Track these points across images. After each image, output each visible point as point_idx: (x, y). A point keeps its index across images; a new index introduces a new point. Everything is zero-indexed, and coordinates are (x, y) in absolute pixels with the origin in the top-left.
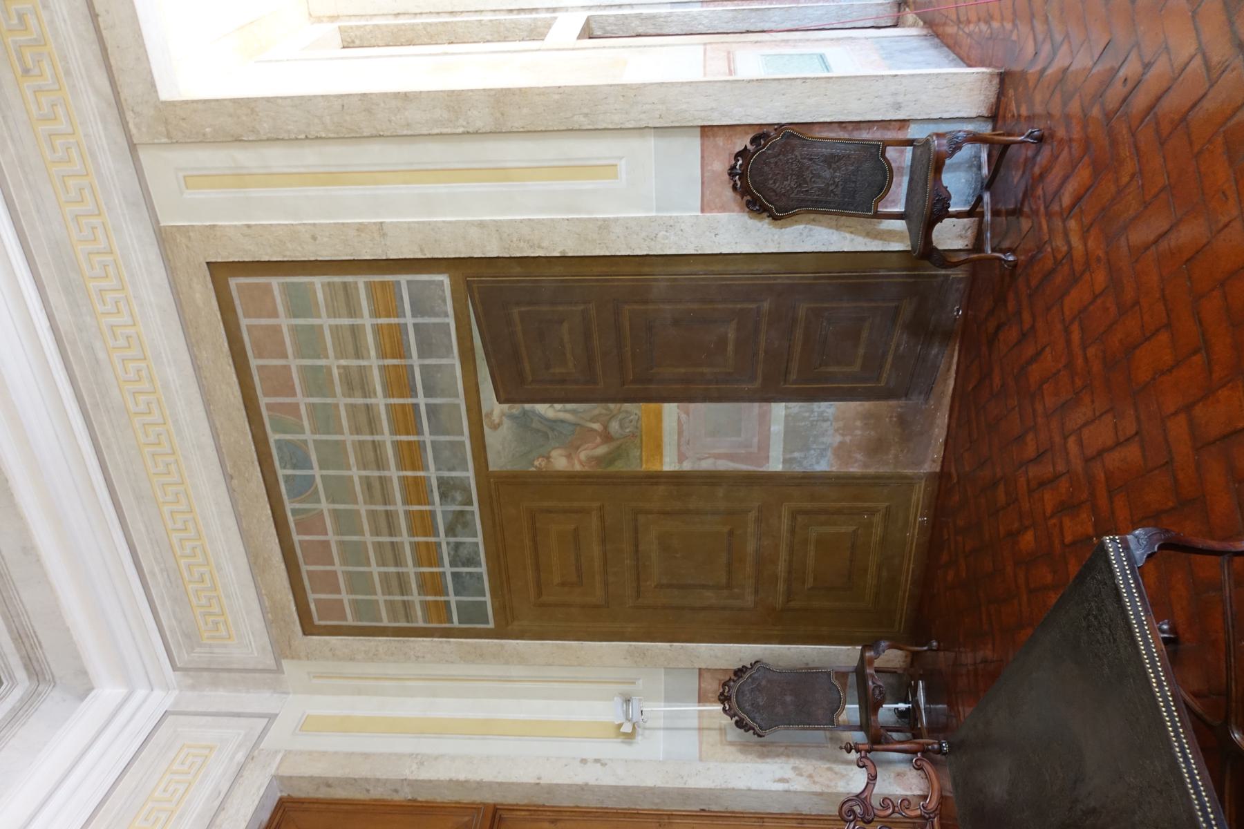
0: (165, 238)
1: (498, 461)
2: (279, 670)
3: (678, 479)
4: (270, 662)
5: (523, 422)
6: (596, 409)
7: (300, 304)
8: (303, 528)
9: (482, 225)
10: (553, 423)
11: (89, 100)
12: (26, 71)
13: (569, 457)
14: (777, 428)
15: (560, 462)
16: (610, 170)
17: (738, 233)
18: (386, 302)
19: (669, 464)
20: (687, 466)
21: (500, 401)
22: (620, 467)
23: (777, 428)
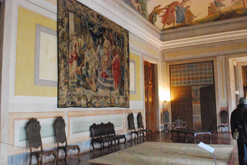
0: (216, 56)
1: (193, 87)
2: (164, 61)
3: (192, 106)
4: (165, 61)
5: (197, 90)
6: (199, 97)
7: (209, 69)
8: (183, 66)
9: (218, 87)
10: (198, 93)
11: (228, 52)
12: (231, 46)
13: (194, 95)
14: (198, 115)
15: (193, 94)
16: (224, 99)
17: (218, 110)
18: (210, 77)
19: (193, 105)
20: (193, 107)
21: (200, 88)
22: (193, 100)
23: (198, 115)
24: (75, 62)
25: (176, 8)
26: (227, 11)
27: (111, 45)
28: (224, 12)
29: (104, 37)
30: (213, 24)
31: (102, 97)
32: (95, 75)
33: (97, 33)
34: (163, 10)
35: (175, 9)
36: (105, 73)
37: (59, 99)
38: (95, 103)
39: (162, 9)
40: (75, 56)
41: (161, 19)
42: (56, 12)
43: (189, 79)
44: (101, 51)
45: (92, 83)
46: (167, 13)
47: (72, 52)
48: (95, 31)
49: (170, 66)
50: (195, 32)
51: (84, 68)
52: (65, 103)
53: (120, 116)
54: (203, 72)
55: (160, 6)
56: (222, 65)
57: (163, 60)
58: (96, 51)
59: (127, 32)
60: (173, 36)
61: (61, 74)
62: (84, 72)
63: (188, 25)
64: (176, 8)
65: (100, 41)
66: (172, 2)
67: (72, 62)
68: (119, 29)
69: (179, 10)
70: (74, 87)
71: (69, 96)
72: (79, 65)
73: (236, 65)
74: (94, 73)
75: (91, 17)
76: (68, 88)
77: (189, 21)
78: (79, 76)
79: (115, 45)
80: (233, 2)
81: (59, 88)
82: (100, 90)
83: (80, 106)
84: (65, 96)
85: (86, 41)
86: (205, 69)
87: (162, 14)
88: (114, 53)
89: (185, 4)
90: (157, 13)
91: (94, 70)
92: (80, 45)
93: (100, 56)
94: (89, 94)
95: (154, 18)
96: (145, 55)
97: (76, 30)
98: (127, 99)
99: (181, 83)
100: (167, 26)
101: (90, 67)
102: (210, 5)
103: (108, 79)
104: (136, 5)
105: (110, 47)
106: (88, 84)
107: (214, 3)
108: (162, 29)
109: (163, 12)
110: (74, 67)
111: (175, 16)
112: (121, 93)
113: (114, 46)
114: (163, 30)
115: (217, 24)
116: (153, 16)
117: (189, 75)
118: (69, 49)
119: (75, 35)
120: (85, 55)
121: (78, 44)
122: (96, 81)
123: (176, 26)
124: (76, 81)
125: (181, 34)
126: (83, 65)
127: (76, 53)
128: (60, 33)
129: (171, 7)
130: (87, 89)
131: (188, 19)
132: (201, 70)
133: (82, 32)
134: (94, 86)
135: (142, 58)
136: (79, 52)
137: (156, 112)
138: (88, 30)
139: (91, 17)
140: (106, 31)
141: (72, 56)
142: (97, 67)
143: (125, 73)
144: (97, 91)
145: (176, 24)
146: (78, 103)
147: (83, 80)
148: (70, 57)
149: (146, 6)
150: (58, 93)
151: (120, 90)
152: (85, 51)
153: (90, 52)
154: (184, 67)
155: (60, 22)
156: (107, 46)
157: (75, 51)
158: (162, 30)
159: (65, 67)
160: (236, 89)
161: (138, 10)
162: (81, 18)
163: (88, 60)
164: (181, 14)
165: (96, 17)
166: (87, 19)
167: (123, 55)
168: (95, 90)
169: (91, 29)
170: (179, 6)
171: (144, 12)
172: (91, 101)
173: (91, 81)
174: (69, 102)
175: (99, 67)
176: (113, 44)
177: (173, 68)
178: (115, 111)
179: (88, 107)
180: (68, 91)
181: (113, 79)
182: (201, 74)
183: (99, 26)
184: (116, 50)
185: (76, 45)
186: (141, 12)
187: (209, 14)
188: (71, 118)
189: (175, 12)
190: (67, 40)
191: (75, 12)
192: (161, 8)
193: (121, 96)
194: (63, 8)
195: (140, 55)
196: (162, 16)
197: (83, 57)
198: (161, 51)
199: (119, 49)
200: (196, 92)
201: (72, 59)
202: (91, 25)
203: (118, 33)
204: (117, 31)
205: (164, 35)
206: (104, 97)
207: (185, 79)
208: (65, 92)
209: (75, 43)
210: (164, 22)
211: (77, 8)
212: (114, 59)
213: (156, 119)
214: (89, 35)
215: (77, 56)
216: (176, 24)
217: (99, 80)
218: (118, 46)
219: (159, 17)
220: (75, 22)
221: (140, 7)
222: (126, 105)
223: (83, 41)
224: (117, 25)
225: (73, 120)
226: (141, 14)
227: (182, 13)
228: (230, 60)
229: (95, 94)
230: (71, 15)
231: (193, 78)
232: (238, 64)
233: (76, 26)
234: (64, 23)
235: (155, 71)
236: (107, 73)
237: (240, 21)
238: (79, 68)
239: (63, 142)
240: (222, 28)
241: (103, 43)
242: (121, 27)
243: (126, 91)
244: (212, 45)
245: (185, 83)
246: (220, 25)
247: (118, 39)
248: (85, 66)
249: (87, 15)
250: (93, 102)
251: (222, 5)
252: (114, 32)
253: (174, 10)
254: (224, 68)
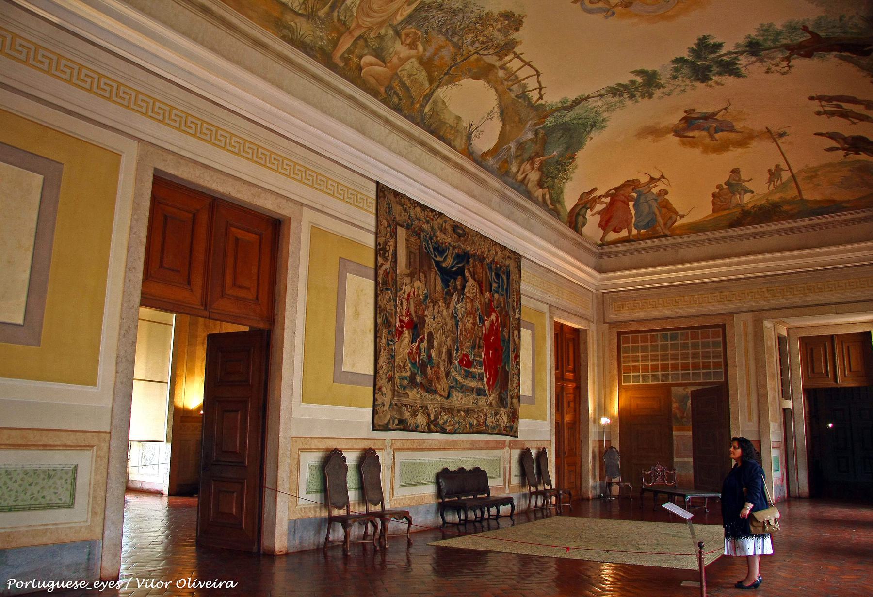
0: (731, 314)
1: (674, 389)
2: (604, 323)
3: (671, 435)
4: (607, 320)
6: (690, 415)
7: (715, 344)
8: (652, 336)
11: (762, 303)
13: (678, 408)
14: (686, 460)
15: (674, 405)
16: (750, 419)
18: (717, 365)
23: (686, 460)
24: (406, 334)
25: (635, 195)
26: (759, 204)
27: (481, 292)
28: (750, 206)
29: (467, 274)
30: (725, 234)
31: (459, 411)
33: (452, 267)
34: (603, 199)
35: (632, 197)
36: (466, 355)
37: (375, 413)
38: (445, 422)
39: (600, 197)
40: (406, 319)
41: (598, 218)
42: (374, 230)
43: (665, 367)
44: (458, 306)
45: (438, 378)
46: (611, 204)
47: (402, 312)
48: (448, 263)
49: (619, 334)
50: (682, 252)
51: (424, 345)
52: (386, 421)
53: (497, 453)
54: (700, 351)
55: (595, 189)
56: (746, 335)
57: (602, 319)
58: (448, 308)
59: (517, 258)
60: (626, 260)
61: (382, 361)
63: (666, 236)
64: (635, 195)
65: (458, 283)
66: (622, 182)
67: (401, 333)
68: (500, 253)
69: (642, 199)
70: (404, 388)
71: (396, 407)
72: (413, 340)
73: (785, 333)
74: (444, 356)
75: (439, 234)
76: (393, 390)
77: (665, 224)
78: (413, 364)
79: (490, 291)
80: (772, 186)
81: (377, 390)
82: (457, 395)
83: (415, 430)
84: (386, 408)
86: (706, 345)
87: (599, 207)
88: (488, 309)
89: (656, 186)
90: (588, 206)
91: (444, 350)
92: (418, 295)
93: (456, 317)
94: (434, 402)
95: (580, 218)
96: (558, 308)
97: (409, 263)
98: (514, 416)
99: (644, 378)
100: (612, 236)
101: (435, 343)
102: (717, 190)
103: (472, 370)
104: (539, 193)
106: (430, 382)
107: (725, 187)
108: (600, 242)
109: (603, 203)
110: (404, 345)
111: (633, 212)
112: (502, 402)
113: (488, 294)
114: (604, 244)
115: (736, 233)
116: (578, 214)
117: (664, 358)
118: (395, 307)
119: (408, 275)
122: (447, 374)
123: (633, 236)
124: (408, 374)
125: (647, 257)
126: (422, 341)
127: (409, 314)
128: (381, 273)
129: (622, 192)
130: (428, 391)
131: (663, 219)
132: (695, 346)
133: (421, 265)
134: (442, 386)
135: (551, 317)
137: (581, 450)
139: (439, 234)
140: (471, 260)
141: (401, 321)
142: (449, 342)
143: (512, 356)
144: (449, 395)
145: (634, 232)
146: (411, 421)
147: (423, 376)
148: (398, 323)
149: (562, 192)
150: (375, 400)
151: (499, 395)
152: (427, 307)
153: (436, 311)
154: (653, 339)
155: (380, 250)
156: (471, 295)
157: (408, 310)
158: (600, 245)
159: (388, 344)
160: (785, 395)
161: (543, 204)
162: (419, 238)
163: (431, 329)
164: (645, 209)
165: (450, 230)
166: (431, 239)
167: (507, 314)
168: (445, 394)
169: (438, 259)
170: (642, 189)
171: (556, 207)
172: (436, 419)
173: (437, 374)
174: (393, 418)
175: (454, 341)
176: (484, 289)
177: (626, 341)
178: (487, 441)
179: (430, 431)
180: (394, 396)
181: (483, 371)
182: (695, 355)
183: (456, 251)
184: (491, 301)
185: (409, 295)
186: (551, 207)
187: (714, 211)
188: (397, 454)
189: (631, 204)
191: (408, 225)
192: (597, 194)
194: (387, 220)
195: (545, 308)
196: (599, 213)
197: (422, 320)
198: (597, 296)
199: (498, 301)
200: (683, 400)
201: (402, 326)
202: (440, 250)
203: (496, 263)
204: (496, 259)
205: (602, 258)
206: (464, 411)
207: (655, 368)
208: (387, 399)
210: (604, 225)
211: (412, 215)
212: (487, 324)
213: (580, 467)
214: (436, 273)
215: (411, 320)
216: (634, 232)
217: (453, 373)
218: (497, 292)
219: (593, 215)
220: (408, 247)
221: (547, 196)
222: (512, 430)
223: (424, 286)
224: (496, 244)
225: (402, 457)
226: (549, 211)
227: (650, 206)
228: (767, 324)
229: (446, 403)
230: (402, 233)
231: (675, 367)
232: (791, 331)
233: (409, 254)
234: (388, 251)
235: (582, 346)
236: (469, 354)
237: (791, 230)
238: (415, 345)
239: (376, 504)
240: (747, 244)
241: (464, 287)
242: (503, 248)
243: (512, 398)
244: (720, 287)
245: (655, 378)
246: (743, 237)
247: (498, 276)
248: (426, 341)
249: (432, 228)
250: (441, 422)
251: (746, 191)
252: (488, 261)
253: (631, 199)
254: (751, 344)
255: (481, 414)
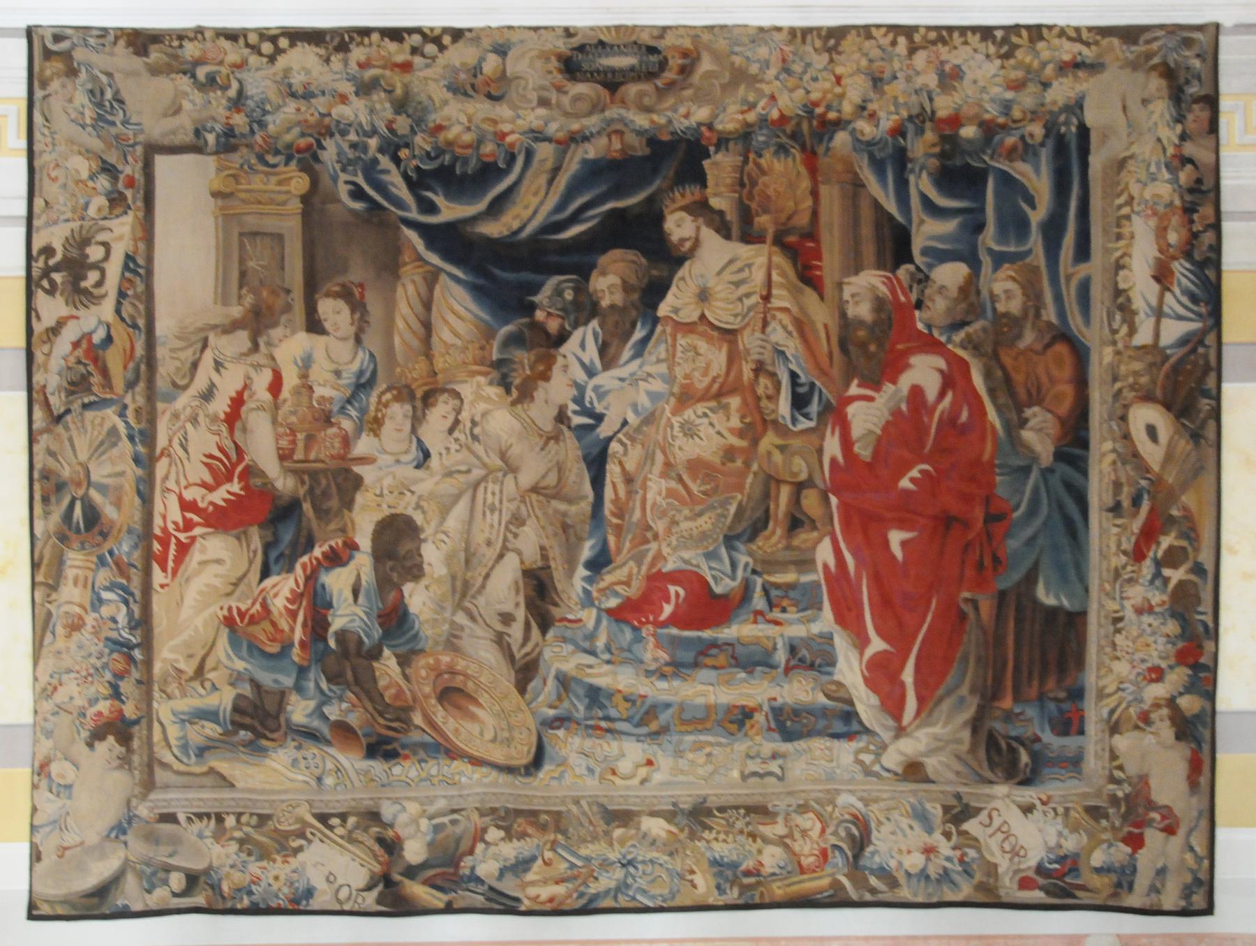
32: (521, 614)
62: (348, 615)
85: (373, 341)
105: (781, 298)
120: (363, 460)
121: (276, 386)
136: (284, 456)
138: (412, 235)
190: (130, 385)
193: (1001, 790)
209: (229, 384)
234: (99, 266)
243: (1114, 729)
255: (808, 821)
